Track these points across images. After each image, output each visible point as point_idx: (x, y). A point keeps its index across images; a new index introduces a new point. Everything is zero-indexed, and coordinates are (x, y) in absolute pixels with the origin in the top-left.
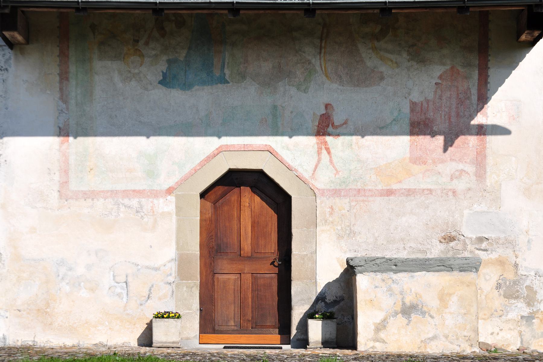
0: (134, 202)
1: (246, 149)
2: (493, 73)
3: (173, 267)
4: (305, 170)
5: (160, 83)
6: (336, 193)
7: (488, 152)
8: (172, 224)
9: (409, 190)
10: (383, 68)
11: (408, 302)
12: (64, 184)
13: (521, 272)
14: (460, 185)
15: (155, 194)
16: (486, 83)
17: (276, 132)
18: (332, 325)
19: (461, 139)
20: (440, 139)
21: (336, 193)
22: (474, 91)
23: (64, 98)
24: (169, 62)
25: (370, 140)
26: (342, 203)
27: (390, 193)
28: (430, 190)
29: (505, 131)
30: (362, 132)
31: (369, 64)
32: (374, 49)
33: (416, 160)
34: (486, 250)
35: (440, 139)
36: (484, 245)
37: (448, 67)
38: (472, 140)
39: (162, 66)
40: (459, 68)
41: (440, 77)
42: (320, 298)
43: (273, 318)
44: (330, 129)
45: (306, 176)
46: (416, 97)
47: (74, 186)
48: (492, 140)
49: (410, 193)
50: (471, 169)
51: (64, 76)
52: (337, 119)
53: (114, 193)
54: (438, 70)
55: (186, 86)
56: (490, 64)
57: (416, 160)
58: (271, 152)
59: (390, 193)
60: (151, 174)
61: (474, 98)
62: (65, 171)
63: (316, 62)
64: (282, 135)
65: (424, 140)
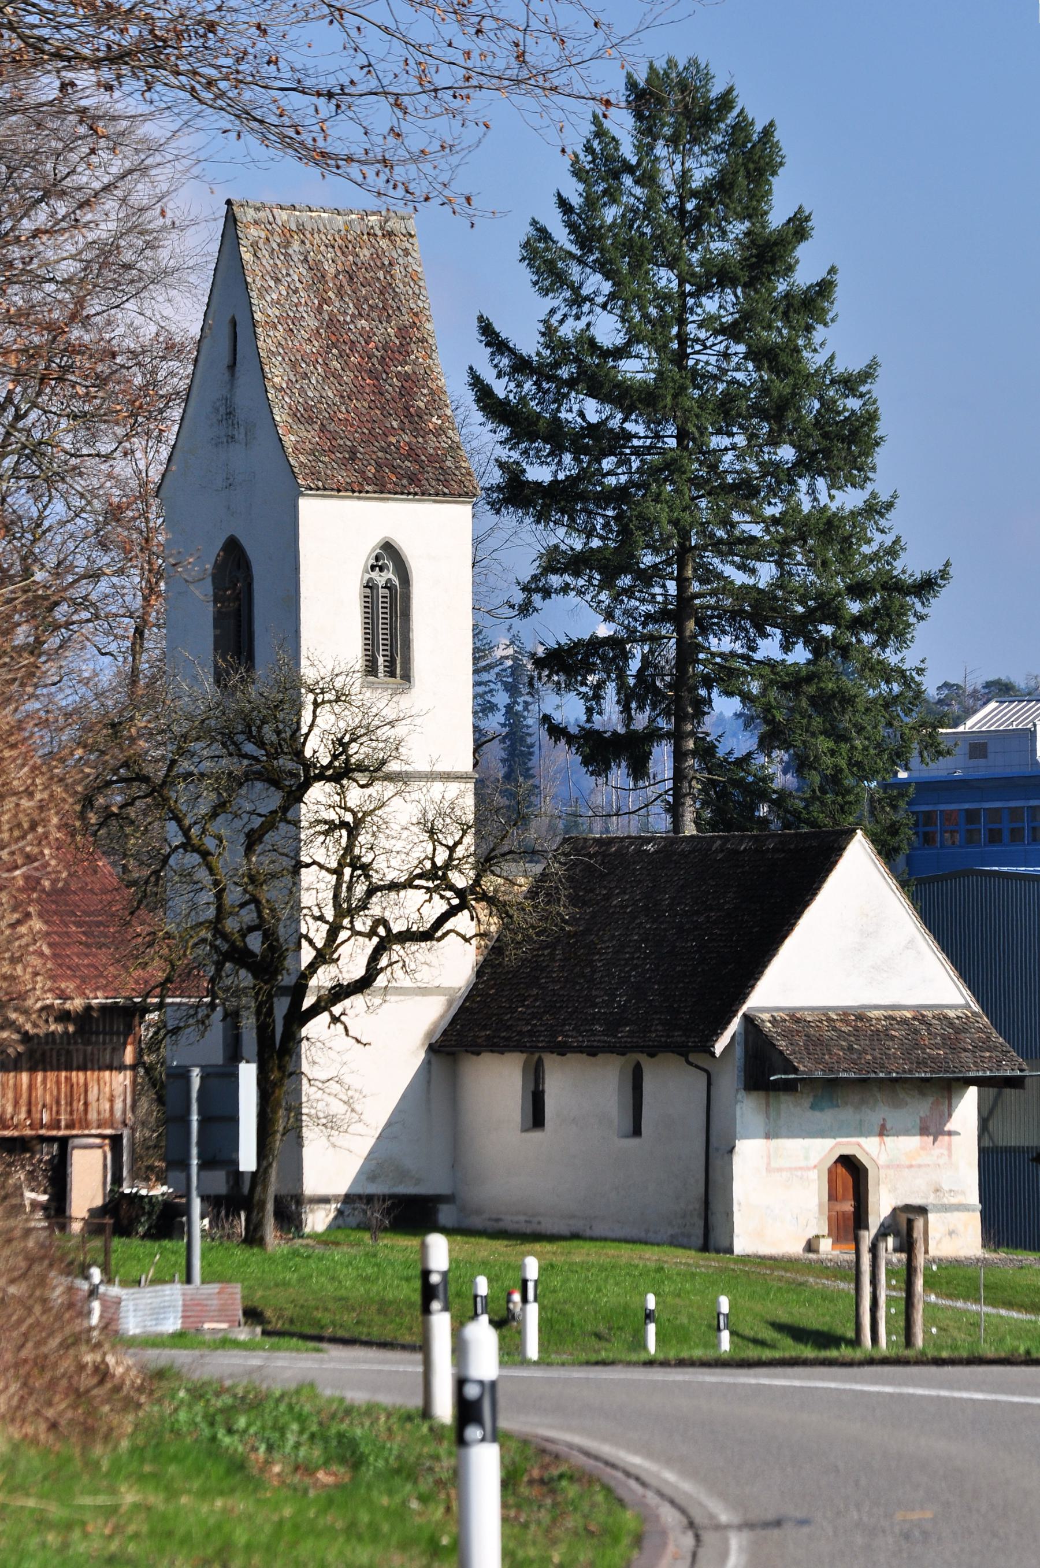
0: (799, 1173)
1: (848, 1143)
2: (954, 1101)
3: (816, 1209)
4: (874, 1155)
6: (888, 1167)
8: (815, 1186)
10: (908, 1099)
11: (951, 1228)
12: (769, 1164)
14: (941, 1161)
15: (808, 1169)
17: (861, 1134)
18: (898, 1240)
19: (940, 1138)
20: (931, 1138)
21: (888, 1167)
23: (768, 1117)
24: (815, 1096)
25: (902, 1139)
26: (891, 1172)
27: (911, 1166)
29: (958, 1134)
30: (897, 1134)
33: (923, 1148)
35: (931, 1138)
38: (946, 1138)
39: (811, 1099)
42: (882, 1225)
43: (852, 1236)
45: (874, 1156)
46: (922, 1114)
47: (773, 1165)
48: (954, 1138)
49: (920, 1166)
50: (946, 1152)
51: (768, 1105)
52: (888, 1127)
53: (790, 1169)
54: (931, 1100)
55: (822, 1110)
57: (923, 1148)
58: (859, 1145)
59: (911, 1166)
60: (807, 1158)
62: (769, 1157)
63: (878, 1095)
65: (925, 1138)
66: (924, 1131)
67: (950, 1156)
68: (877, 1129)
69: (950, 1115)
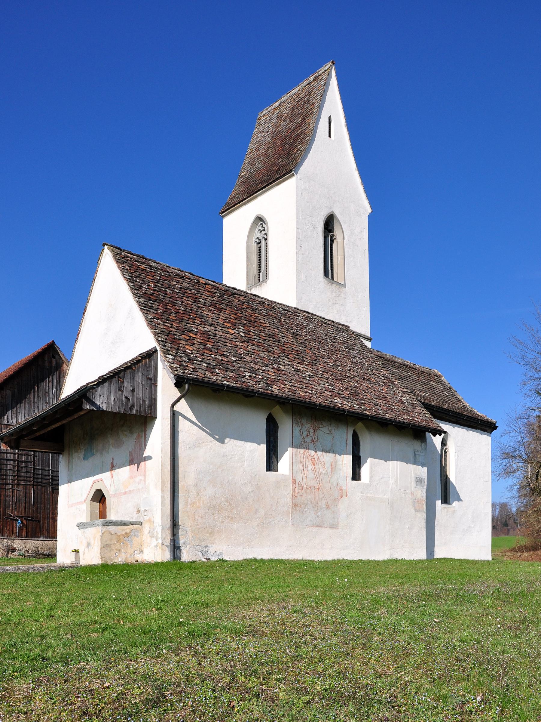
5: (84, 459)
7: (147, 469)
9: (130, 491)
13: (155, 525)
16: (146, 438)
21: (114, 495)
22: (143, 442)
27: (125, 493)
28: (134, 490)
31: (121, 438)
32: (122, 431)
34: (146, 516)
36: (146, 513)
37: (137, 434)
40: (140, 433)
41: (136, 439)
44: (113, 468)
49: (130, 492)
50: (142, 478)
52: (114, 464)
54: (135, 435)
56: (147, 429)
61: (143, 445)
64: (104, 473)
66: (131, 462)
67: (145, 481)
68: (109, 467)
69: (145, 445)
